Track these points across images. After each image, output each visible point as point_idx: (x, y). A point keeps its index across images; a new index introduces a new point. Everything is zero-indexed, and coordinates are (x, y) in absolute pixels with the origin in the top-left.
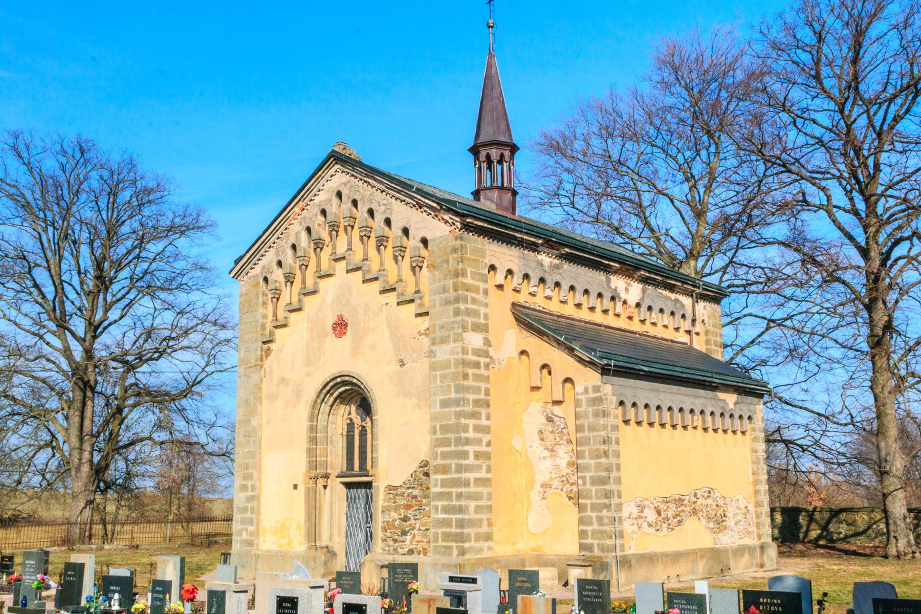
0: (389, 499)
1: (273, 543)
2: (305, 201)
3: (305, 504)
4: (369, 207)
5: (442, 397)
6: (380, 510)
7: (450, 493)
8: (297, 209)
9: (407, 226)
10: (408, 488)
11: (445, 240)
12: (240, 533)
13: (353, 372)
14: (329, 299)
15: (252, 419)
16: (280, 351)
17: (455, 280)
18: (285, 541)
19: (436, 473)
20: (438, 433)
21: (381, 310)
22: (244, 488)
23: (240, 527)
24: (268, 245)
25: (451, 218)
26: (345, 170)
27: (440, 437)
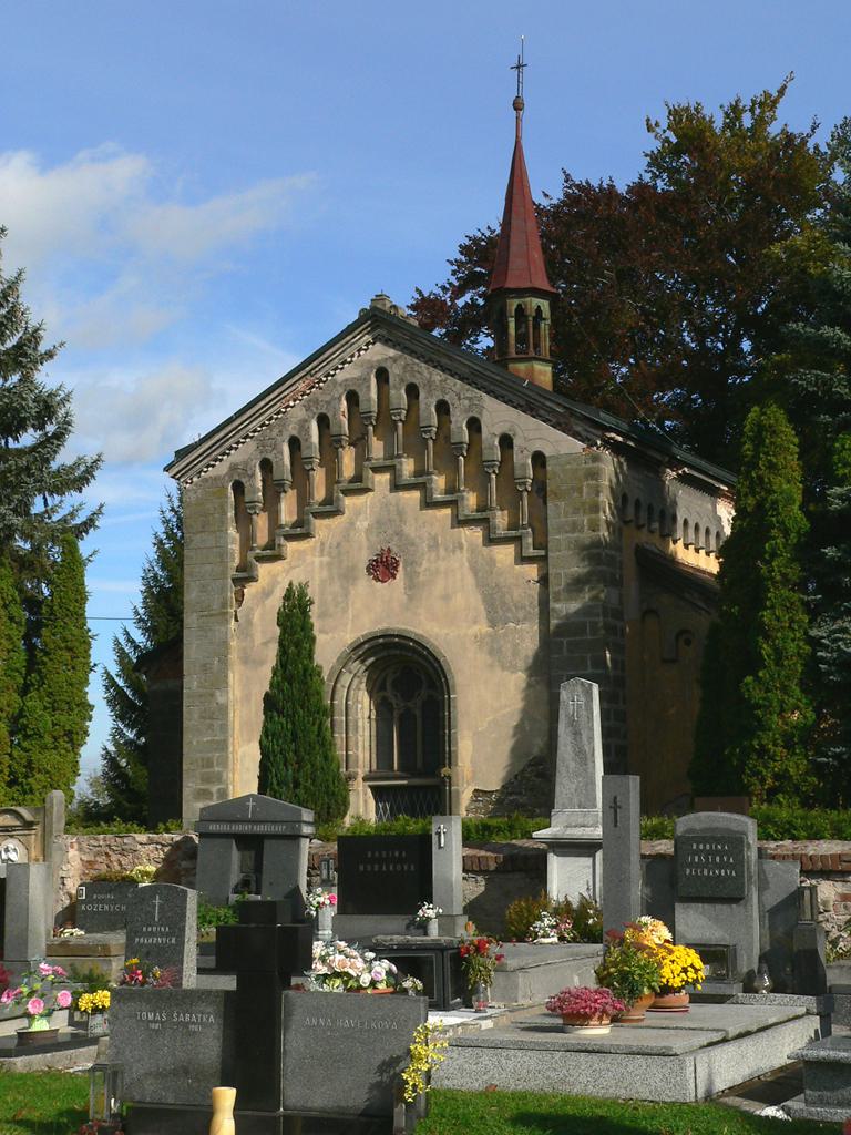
0: (477, 808)
2: (318, 375)
8: (301, 386)
9: (511, 433)
10: (511, 794)
11: (574, 460)
14: (363, 524)
15: (218, 693)
17: (593, 516)
24: (243, 433)
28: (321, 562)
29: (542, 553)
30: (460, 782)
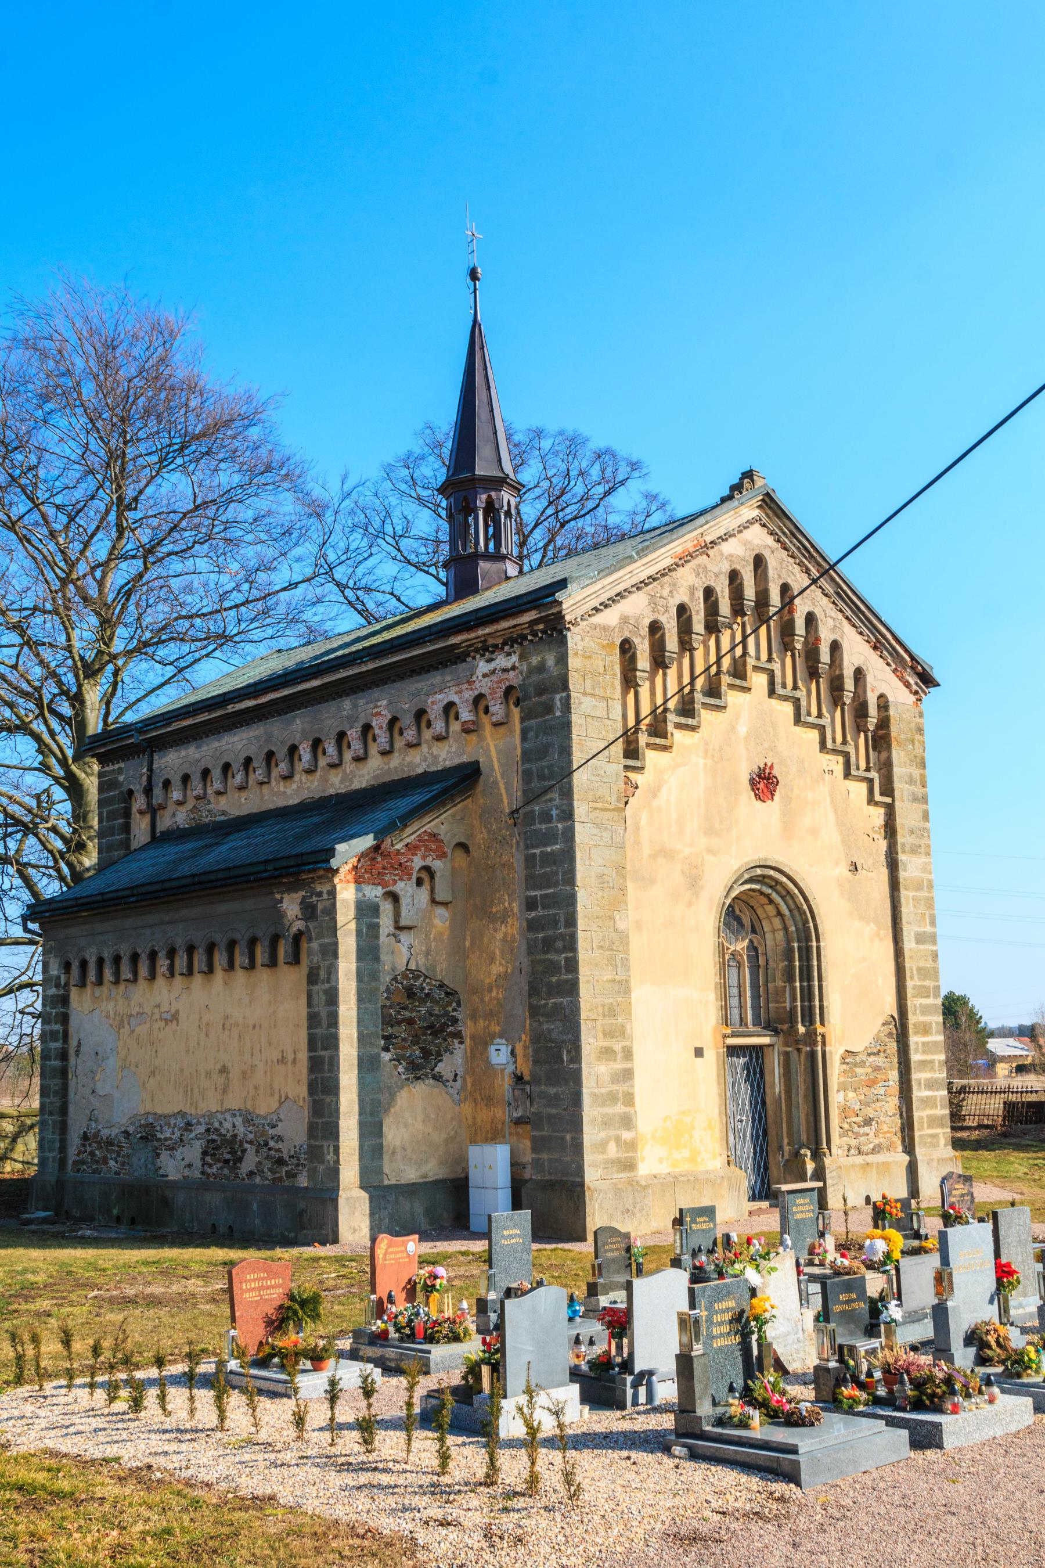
1: (661, 1160)
3: (719, 1083)
4: (811, 609)
5: (917, 929)
6: (836, 1087)
7: (932, 1062)
12: (602, 1146)
13: (785, 865)
16: (654, 793)
18: (686, 1153)
19: (916, 1033)
20: (916, 977)
21: (823, 779)
22: (607, 1053)
23: (603, 1135)
25: (916, 684)
26: (771, 527)
27: (918, 983)
28: (705, 765)
29: (889, 800)
30: (833, 1043)
